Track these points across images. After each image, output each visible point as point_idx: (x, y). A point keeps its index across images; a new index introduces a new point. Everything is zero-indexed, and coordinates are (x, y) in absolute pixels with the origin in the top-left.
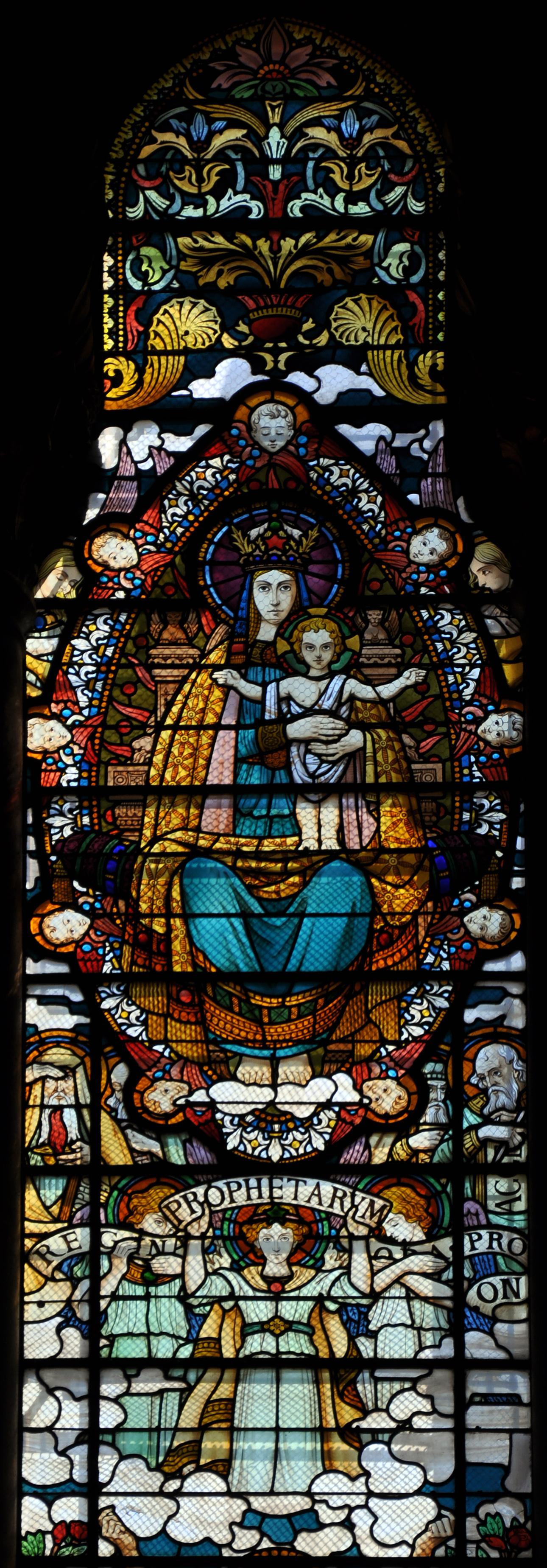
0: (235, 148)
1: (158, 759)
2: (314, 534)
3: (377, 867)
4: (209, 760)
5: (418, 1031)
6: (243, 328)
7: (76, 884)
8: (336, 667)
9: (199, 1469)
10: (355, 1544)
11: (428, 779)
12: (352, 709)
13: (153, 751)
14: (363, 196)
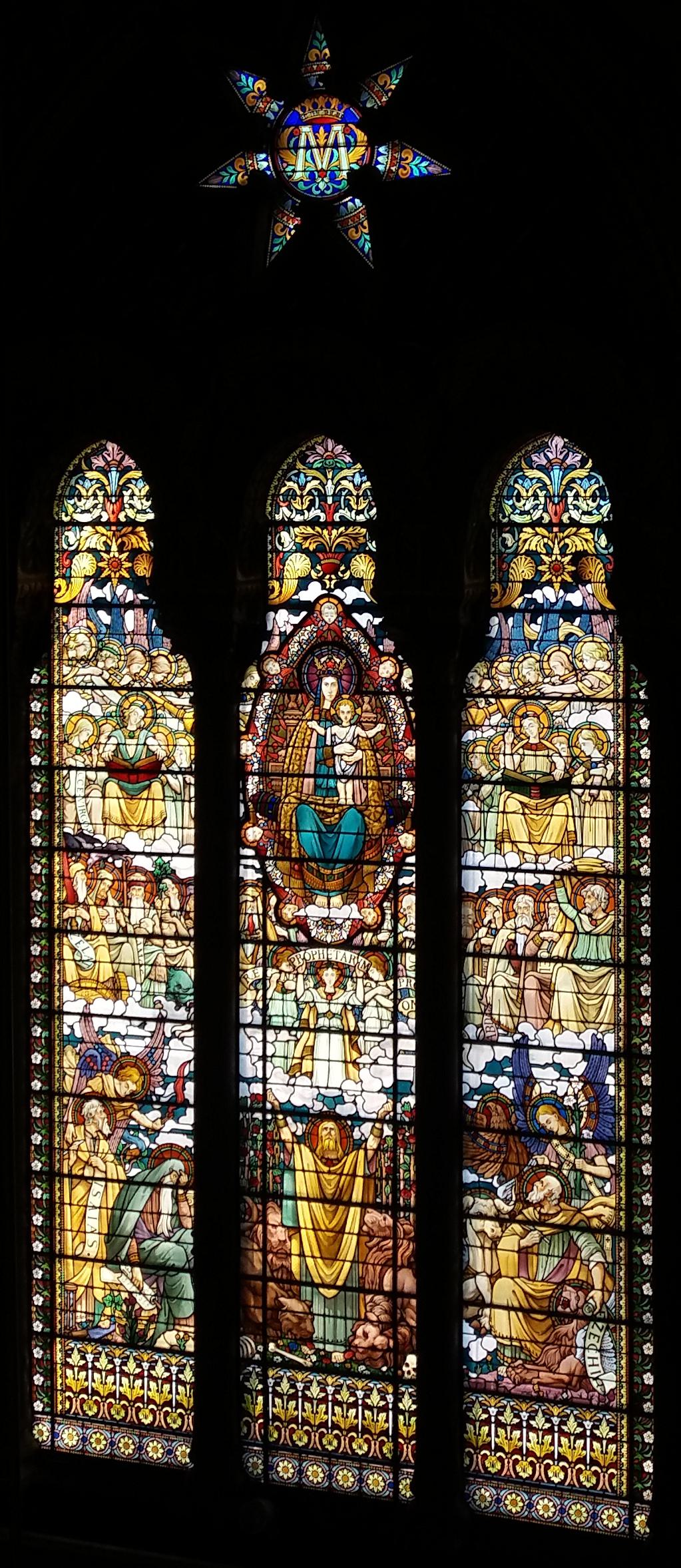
0: (316, 489)
1: (287, 760)
2: (344, 661)
3: (367, 813)
4: (305, 761)
5: (381, 888)
6: (319, 567)
7: (258, 815)
8: (352, 722)
9: (301, 1075)
10: (357, 1112)
11: (386, 774)
12: (358, 741)
13: (285, 757)
14: (362, 512)
